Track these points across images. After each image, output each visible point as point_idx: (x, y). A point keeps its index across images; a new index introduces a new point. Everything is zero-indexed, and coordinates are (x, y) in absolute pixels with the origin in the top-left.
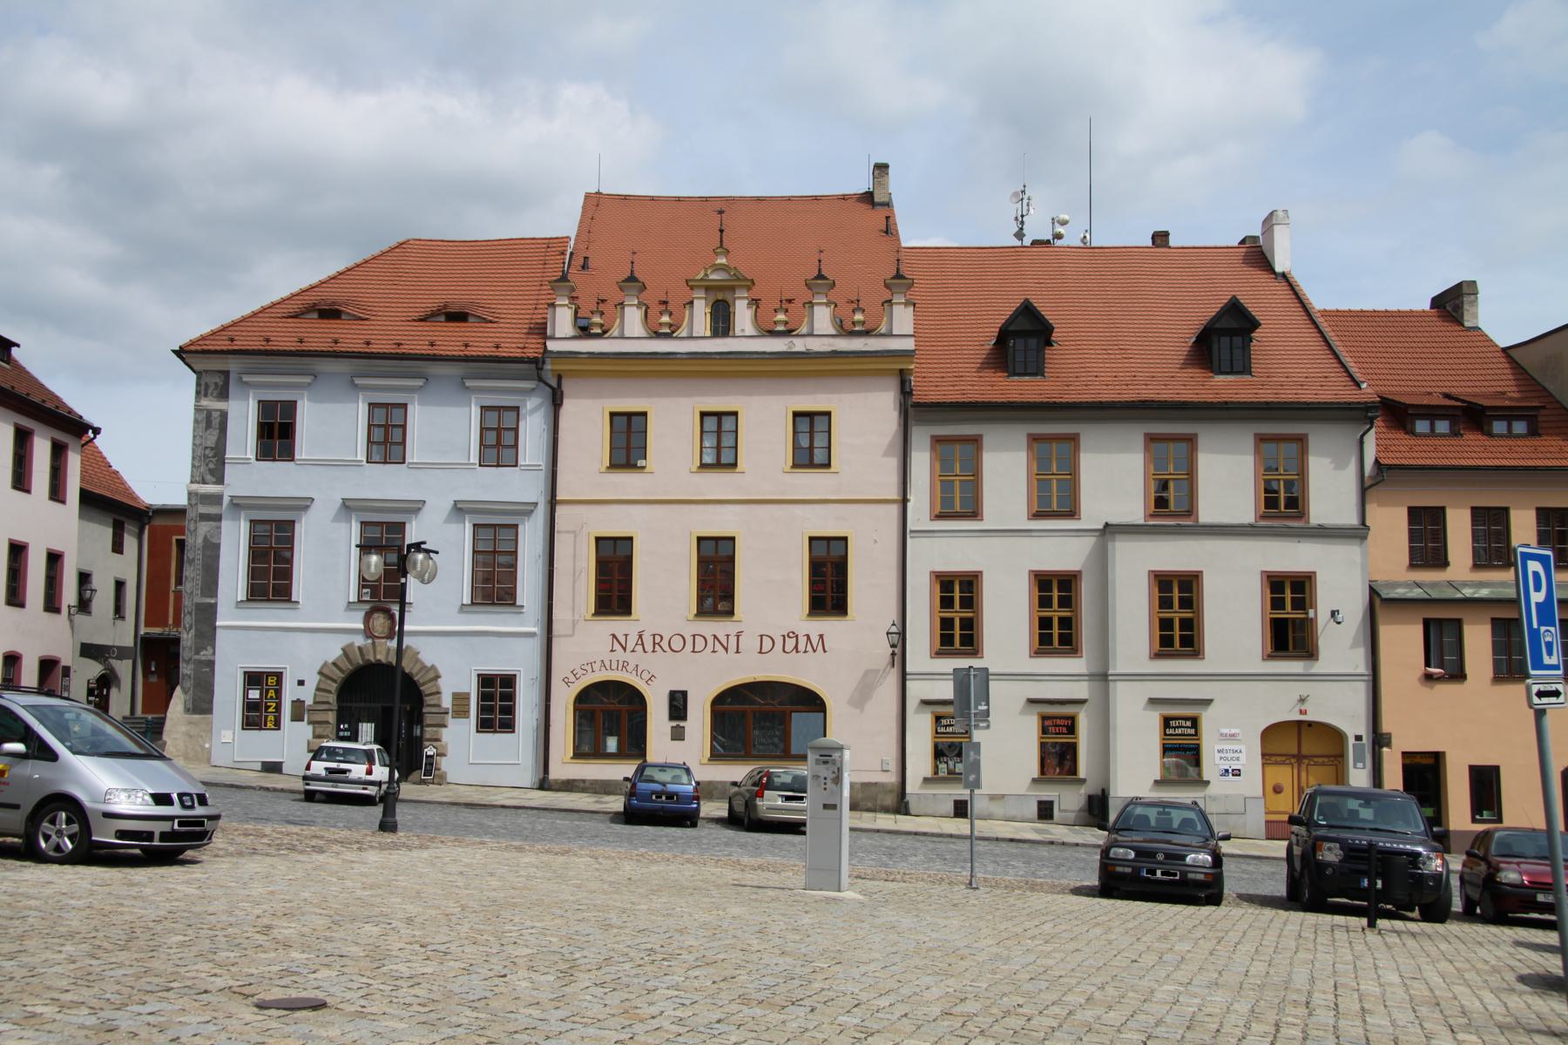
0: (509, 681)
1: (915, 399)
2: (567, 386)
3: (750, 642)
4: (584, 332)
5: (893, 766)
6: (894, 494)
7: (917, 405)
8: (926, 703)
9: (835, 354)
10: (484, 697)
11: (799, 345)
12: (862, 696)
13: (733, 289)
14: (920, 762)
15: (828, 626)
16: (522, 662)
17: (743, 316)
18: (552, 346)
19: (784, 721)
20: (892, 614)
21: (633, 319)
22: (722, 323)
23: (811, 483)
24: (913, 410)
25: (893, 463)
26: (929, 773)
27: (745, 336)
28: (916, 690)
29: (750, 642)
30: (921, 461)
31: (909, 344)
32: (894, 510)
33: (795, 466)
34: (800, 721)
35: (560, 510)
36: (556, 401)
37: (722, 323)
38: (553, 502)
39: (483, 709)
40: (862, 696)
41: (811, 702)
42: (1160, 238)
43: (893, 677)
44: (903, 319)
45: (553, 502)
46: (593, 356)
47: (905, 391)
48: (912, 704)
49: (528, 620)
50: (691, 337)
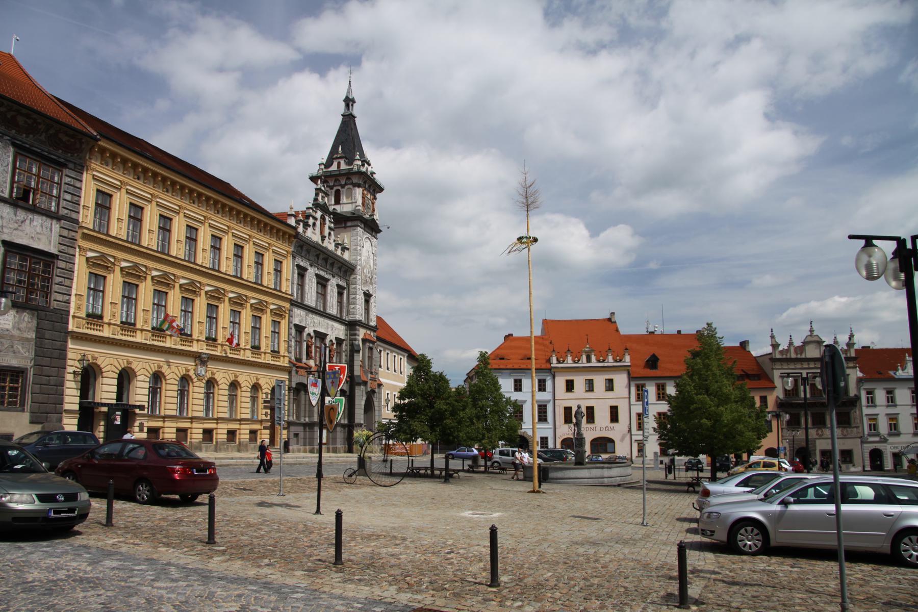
0: (547, 438)
1: (631, 376)
2: (556, 374)
3: (598, 429)
4: (559, 362)
5: (629, 453)
6: (627, 396)
7: (632, 378)
8: (636, 440)
9: (614, 366)
10: (541, 442)
11: (606, 364)
12: (622, 439)
13: (591, 352)
14: (635, 453)
15: (615, 425)
16: (549, 434)
17: (593, 358)
18: (552, 365)
19: (606, 446)
20: (628, 423)
21: (569, 359)
22: (589, 360)
23: (610, 394)
24: (631, 378)
25: (627, 390)
26: (637, 455)
27: (594, 363)
28: (634, 438)
29: (598, 429)
30: (633, 389)
31: (629, 364)
32: (628, 400)
33: (606, 390)
34: (609, 445)
35: (556, 401)
36: (554, 377)
37: (589, 360)
38: (554, 400)
39: (541, 444)
40: (622, 439)
41: (612, 441)
42: (679, 332)
43: (629, 435)
44: (627, 358)
45: (554, 400)
46: (562, 368)
47: (629, 374)
48: (633, 441)
49: (550, 425)
50: (582, 363)
